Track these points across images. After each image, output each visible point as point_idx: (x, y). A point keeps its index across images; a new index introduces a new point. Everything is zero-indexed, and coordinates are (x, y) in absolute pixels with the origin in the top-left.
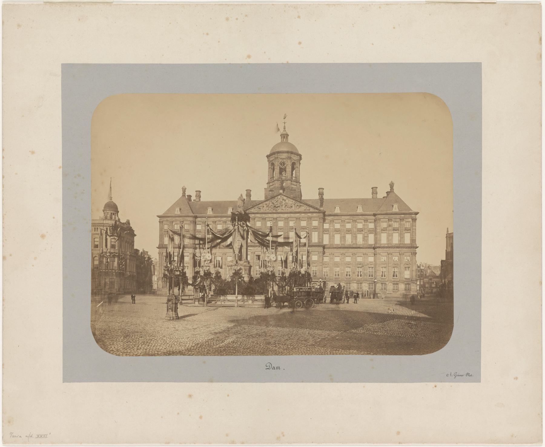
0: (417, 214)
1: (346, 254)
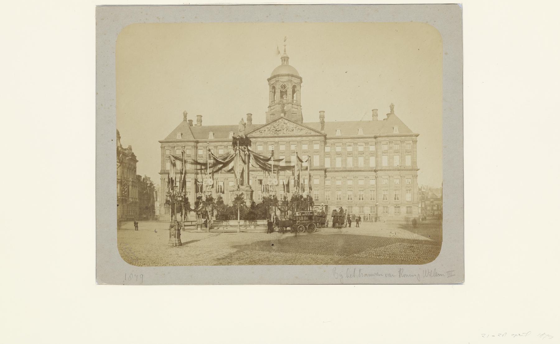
0: (417, 136)
1: (348, 177)
